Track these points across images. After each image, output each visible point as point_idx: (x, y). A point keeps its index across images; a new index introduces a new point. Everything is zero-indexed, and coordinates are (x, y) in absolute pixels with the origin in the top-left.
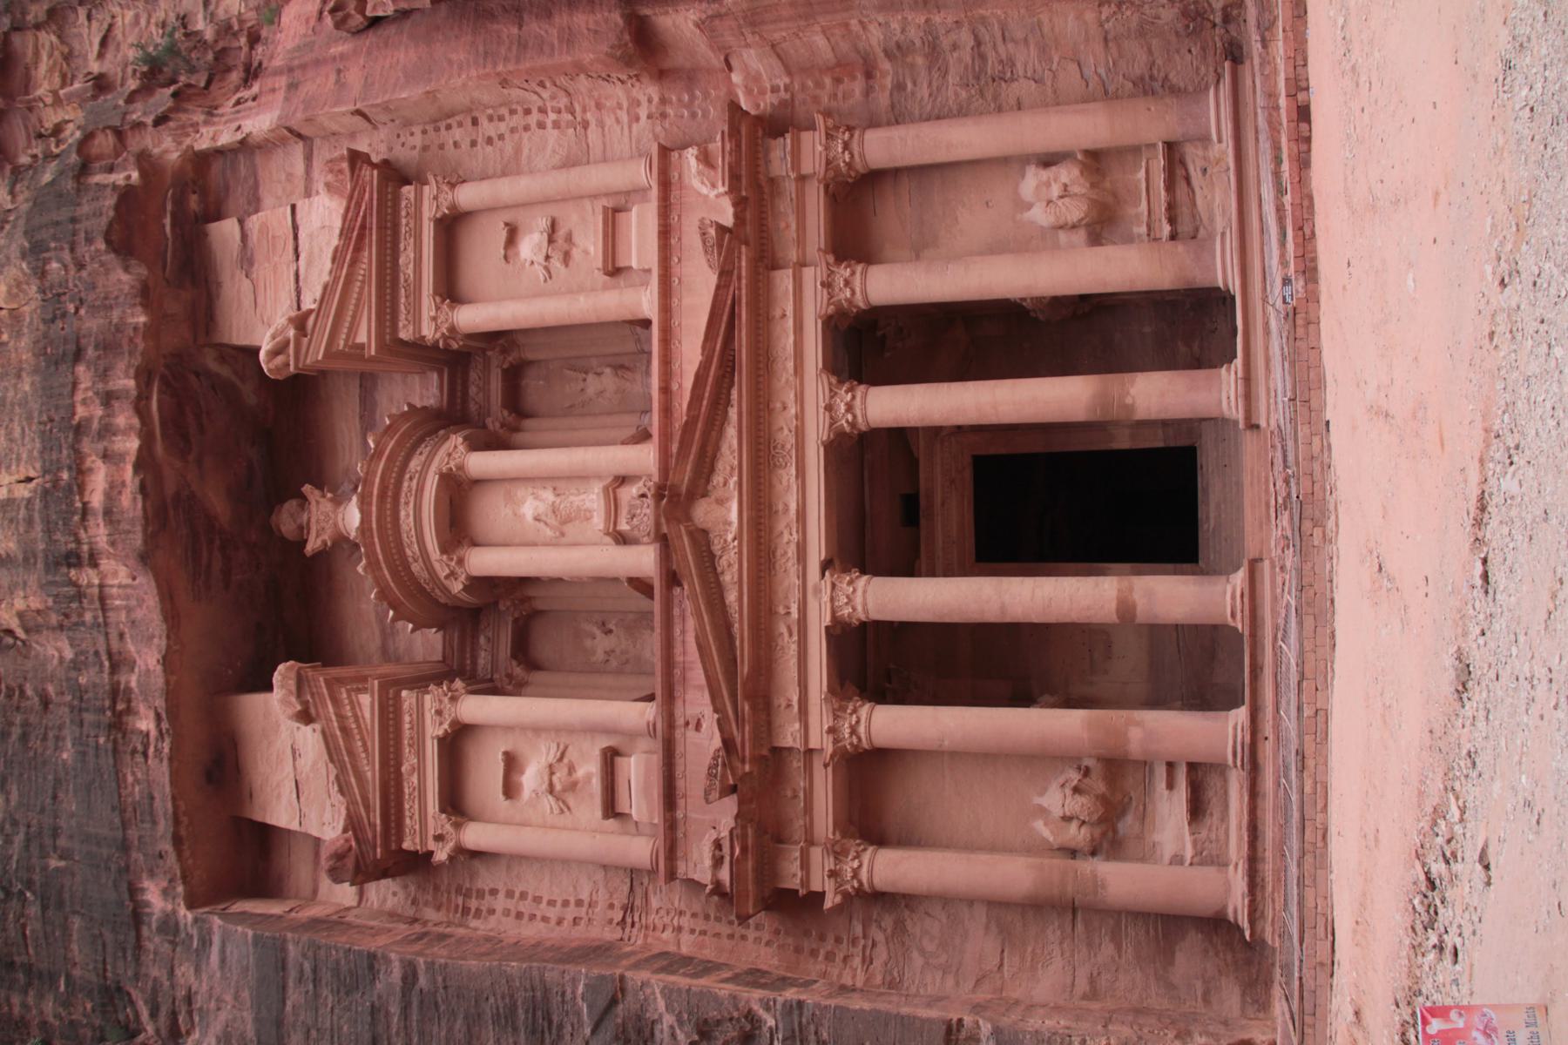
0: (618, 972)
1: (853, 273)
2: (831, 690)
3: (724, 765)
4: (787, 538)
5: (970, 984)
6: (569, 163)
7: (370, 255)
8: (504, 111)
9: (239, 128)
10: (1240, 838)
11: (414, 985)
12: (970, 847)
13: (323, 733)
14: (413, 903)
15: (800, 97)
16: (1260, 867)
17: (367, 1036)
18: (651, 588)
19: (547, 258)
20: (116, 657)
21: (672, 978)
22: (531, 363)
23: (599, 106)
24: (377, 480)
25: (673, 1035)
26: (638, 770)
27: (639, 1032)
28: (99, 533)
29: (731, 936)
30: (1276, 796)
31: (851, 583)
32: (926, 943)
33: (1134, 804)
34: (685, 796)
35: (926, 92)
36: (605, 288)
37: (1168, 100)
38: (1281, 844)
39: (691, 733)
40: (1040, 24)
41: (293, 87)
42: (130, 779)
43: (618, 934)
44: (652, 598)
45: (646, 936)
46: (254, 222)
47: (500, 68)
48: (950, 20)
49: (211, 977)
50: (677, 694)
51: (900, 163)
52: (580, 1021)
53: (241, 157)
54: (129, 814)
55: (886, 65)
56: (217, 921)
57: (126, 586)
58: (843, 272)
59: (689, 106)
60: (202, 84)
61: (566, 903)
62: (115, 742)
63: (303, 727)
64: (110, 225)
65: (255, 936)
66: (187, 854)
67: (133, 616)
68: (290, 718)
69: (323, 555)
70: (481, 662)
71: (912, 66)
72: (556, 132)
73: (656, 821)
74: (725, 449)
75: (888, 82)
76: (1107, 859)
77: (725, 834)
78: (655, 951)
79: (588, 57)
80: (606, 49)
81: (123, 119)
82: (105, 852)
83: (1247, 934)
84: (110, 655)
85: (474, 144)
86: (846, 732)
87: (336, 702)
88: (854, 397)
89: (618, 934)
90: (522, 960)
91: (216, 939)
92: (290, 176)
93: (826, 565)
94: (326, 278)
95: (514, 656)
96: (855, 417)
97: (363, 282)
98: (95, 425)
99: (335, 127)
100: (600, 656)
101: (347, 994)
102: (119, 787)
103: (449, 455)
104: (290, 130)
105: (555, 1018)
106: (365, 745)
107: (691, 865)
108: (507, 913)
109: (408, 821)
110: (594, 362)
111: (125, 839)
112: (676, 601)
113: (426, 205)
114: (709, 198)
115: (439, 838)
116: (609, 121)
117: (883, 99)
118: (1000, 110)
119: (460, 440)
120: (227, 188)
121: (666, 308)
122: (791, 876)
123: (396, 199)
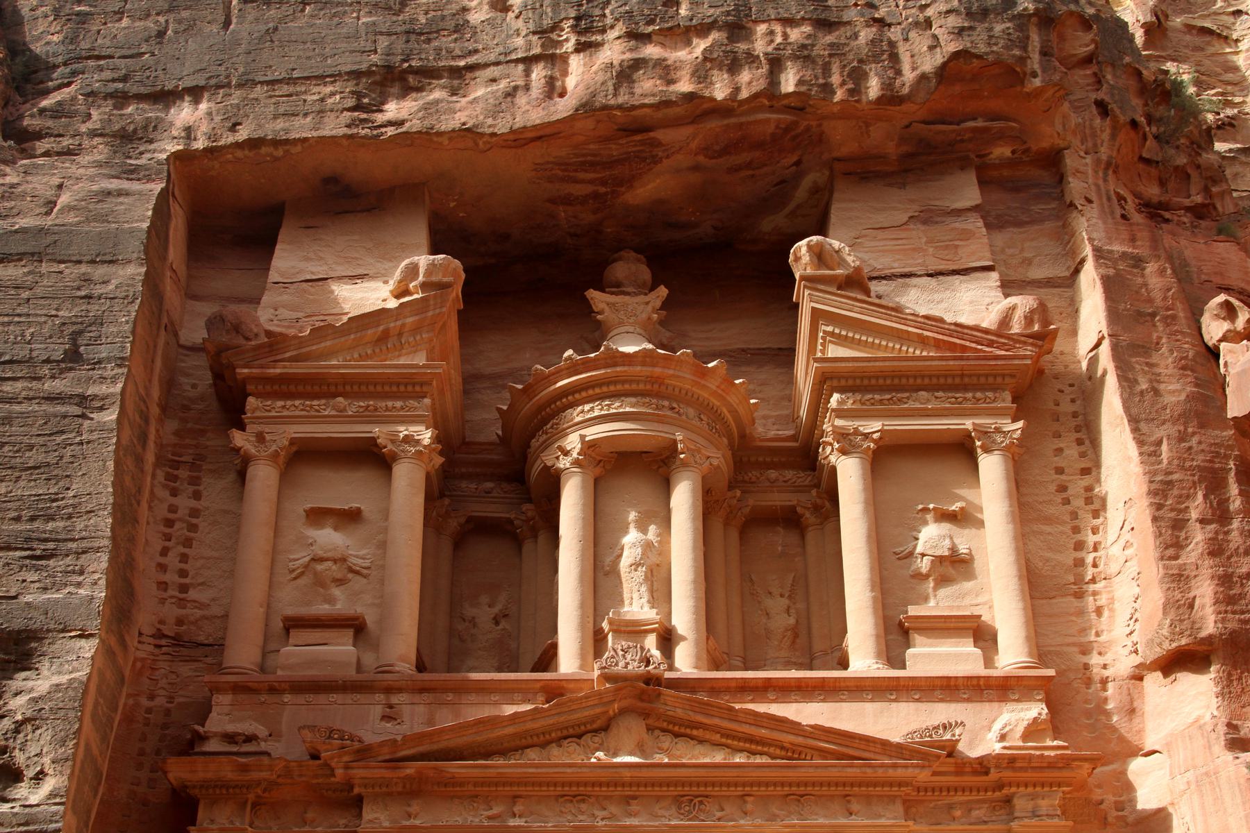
9: (1090, 201)
18: (545, 670)
19: (923, 555)
20: (469, 75)
24: (671, 372)
34: (308, 703)
39: (378, 710)
43: (148, 630)
44: (533, 670)
46: (975, 224)
50: (425, 696)
67: (520, 93)
69: (587, 310)
73: (280, 673)
74: (699, 749)
77: (263, 746)
84: (471, 68)
102: (316, 77)
109: (280, 403)
115: (260, 438)
119: (715, 462)
123: (994, 389)
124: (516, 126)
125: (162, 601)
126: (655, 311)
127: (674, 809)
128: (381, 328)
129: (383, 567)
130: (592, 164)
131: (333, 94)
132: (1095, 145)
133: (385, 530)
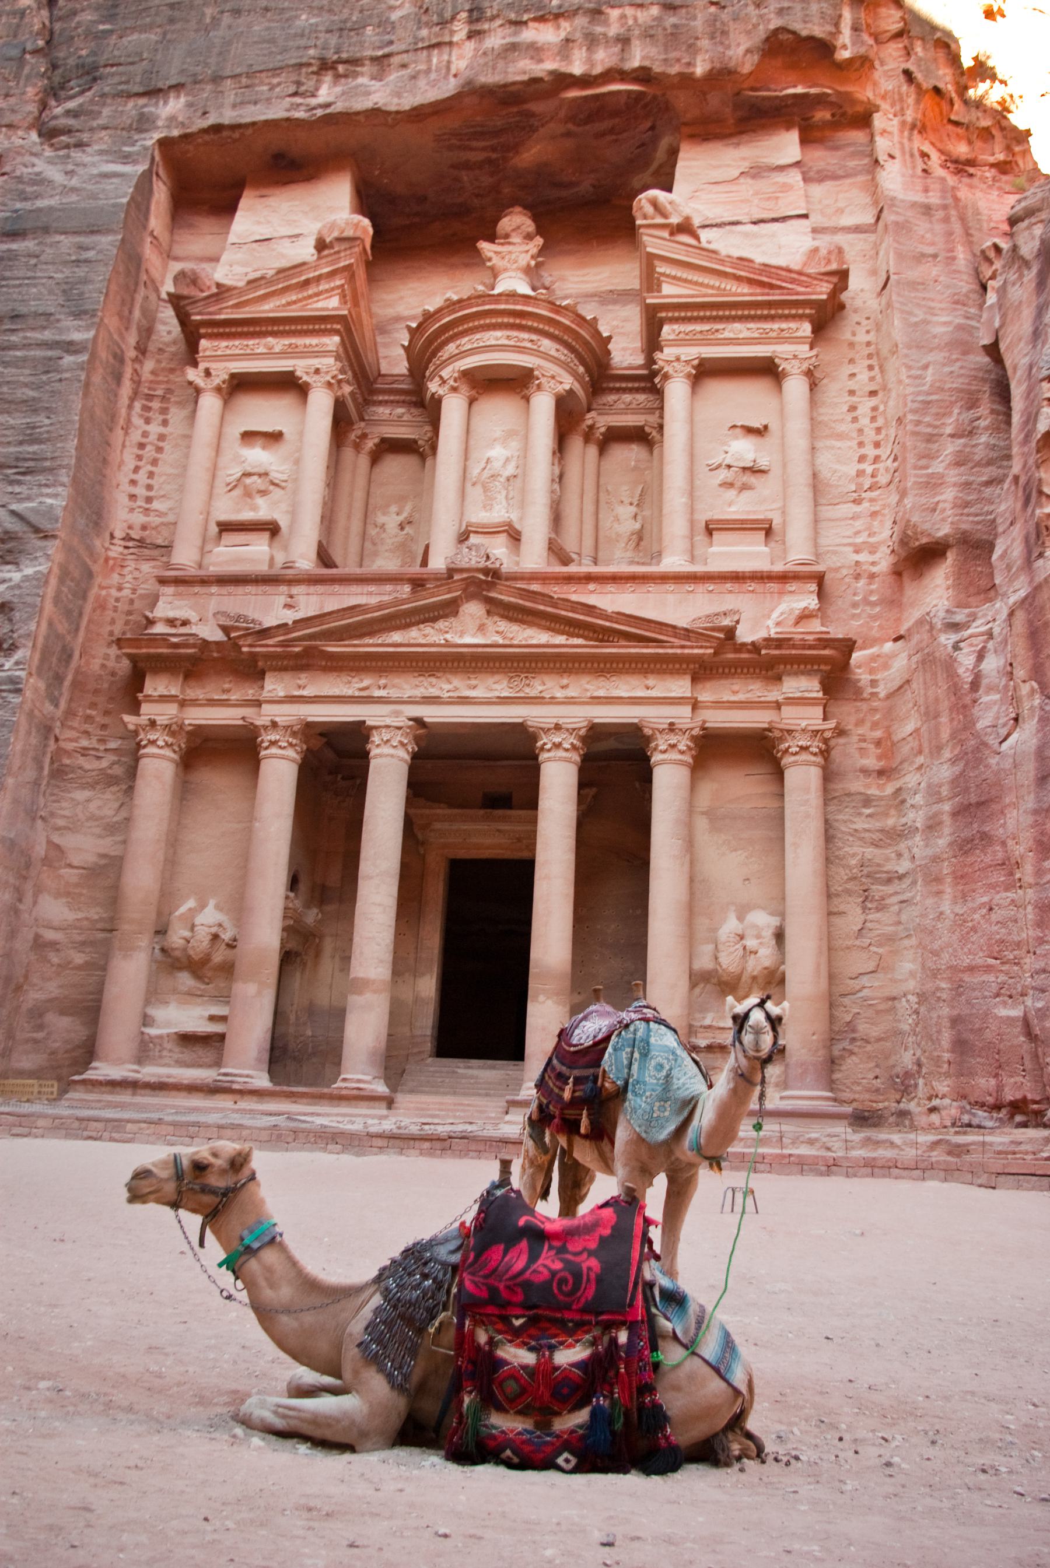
0: (62, 534)
1: (682, 752)
2: (309, 726)
3: (247, 629)
4: (444, 686)
5: (56, 839)
6: (817, 485)
7: (742, 292)
8: (880, 422)
9: (892, 157)
10: (159, 1076)
11: (68, 352)
12: (173, 842)
13: (304, 264)
14: (160, 349)
15: (864, 706)
16: (129, 1091)
17: (23, 309)
19: (729, 467)
20: (386, 62)
21: (53, 581)
22: (651, 452)
23: (874, 514)
25: (4, 581)
26: (255, 553)
27: (10, 551)
28: (497, 39)
29: (111, 633)
30: (185, 1108)
31: (401, 743)
32: (98, 803)
33: (203, 987)
34: (230, 594)
35: (859, 826)
36: (692, 523)
37: (822, 1052)
38: (142, 1108)
39: (282, 600)
40: (908, 936)
41: (927, 210)
42: (275, 81)
43: (119, 534)
45: (114, 559)
46: (795, 177)
47: (910, 417)
48: (915, 850)
49: (94, 164)
50: (320, 588)
51: (787, 798)
52: (21, 500)
53: (866, 161)
54: (244, 80)
55: (889, 790)
56: (141, 168)
57: (448, 68)
58: (684, 743)
59: (866, 601)
60: (953, 117)
61: (149, 487)
62: (310, 65)
63: (312, 242)
64: (794, 33)
65: (122, 205)
66: (207, 138)
68: (319, 233)
70: (381, 410)
71: (887, 815)
72: (854, 473)
75: (873, 791)
76: (153, 960)
77: (194, 630)
78: (95, 568)
79: (908, 502)
80: (915, 519)
81: (918, 38)
82: (212, 60)
83: (76, 1078)
85: (852, 393)
86: (273, 737)
87: (332, 274)
88: (567, 750)
89: (119, 534)
90: (79, 447)
91: (127, 169)
92: (840, 211)
93: (419, 722)
94: (724, 252)
95: (383, 440)
96: (549, 750)
97: (719, 288)
98: (599, 29)
99: (882, 253)
100: (381, 519)
101: (64, 291)
103: (553, 377)
104: (881, 211)
105: (28, 478)
106: (295, 302)
107: (170, 599)
108: (145, 434)
109: (224, 344)
110: (647, 513)
111: (223, 78)
112: (399, 587)
113: (790, 344)
114: (764, 619)
115: (208, 373)
116: (858, 524)
117: (857, 785)
118: (829, 896)
119: (567, 387)
120: (836, 148)
121: (664, 578)
122: (155, 686)
124: (416, 104)
125: (132, 510)
126: (532, 257)
127: (505, 682)
128: (303, 278)
129: (296, 480)
130: (482, 133)
131: (279, 84)
132: (902, 109)
133: (299, 450)
